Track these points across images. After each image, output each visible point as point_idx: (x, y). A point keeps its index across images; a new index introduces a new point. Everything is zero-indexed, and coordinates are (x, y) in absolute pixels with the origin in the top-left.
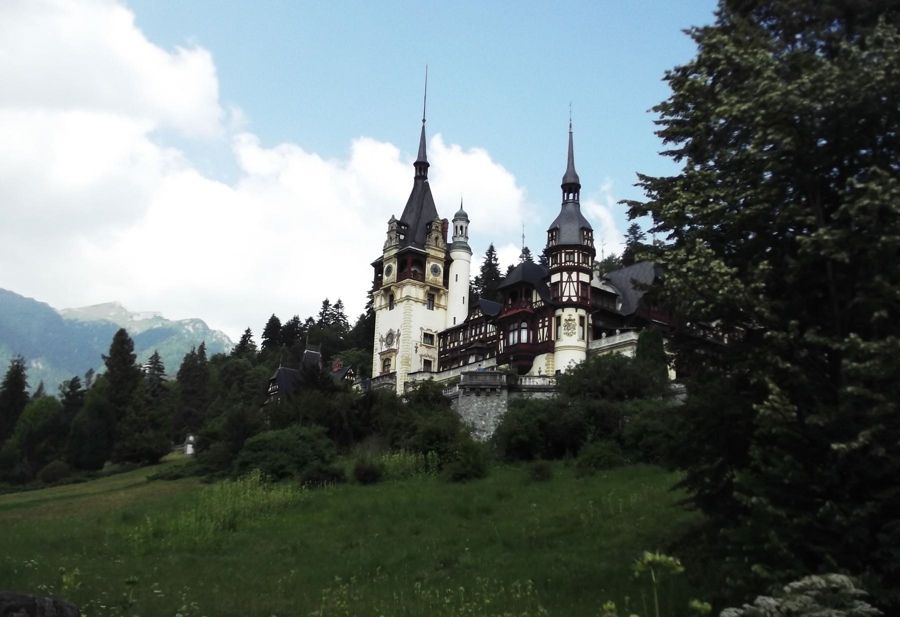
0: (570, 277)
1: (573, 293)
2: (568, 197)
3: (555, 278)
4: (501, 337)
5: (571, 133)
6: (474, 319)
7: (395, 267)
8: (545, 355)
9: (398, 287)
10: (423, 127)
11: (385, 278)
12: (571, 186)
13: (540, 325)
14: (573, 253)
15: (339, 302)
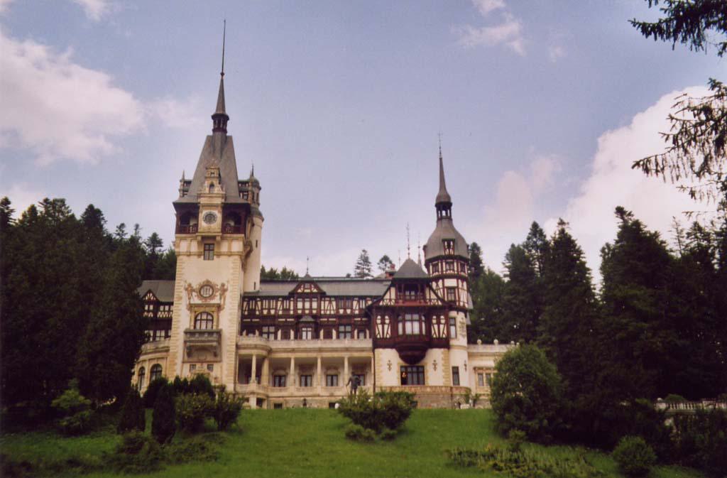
0: (463, 285)
1: (466, 301)
2: (441, 213)
3: (451, 283)
4: (379, 321)
5: (441, 159)
6: (303, 293)
7: (218, 214)
8: (442, 350)
9: (223, 238)
10: (222, 81)
11: (203, 225)
12: (444, 205)
13: (434, 321)
14: (464, 265)
15: (155, 235)
